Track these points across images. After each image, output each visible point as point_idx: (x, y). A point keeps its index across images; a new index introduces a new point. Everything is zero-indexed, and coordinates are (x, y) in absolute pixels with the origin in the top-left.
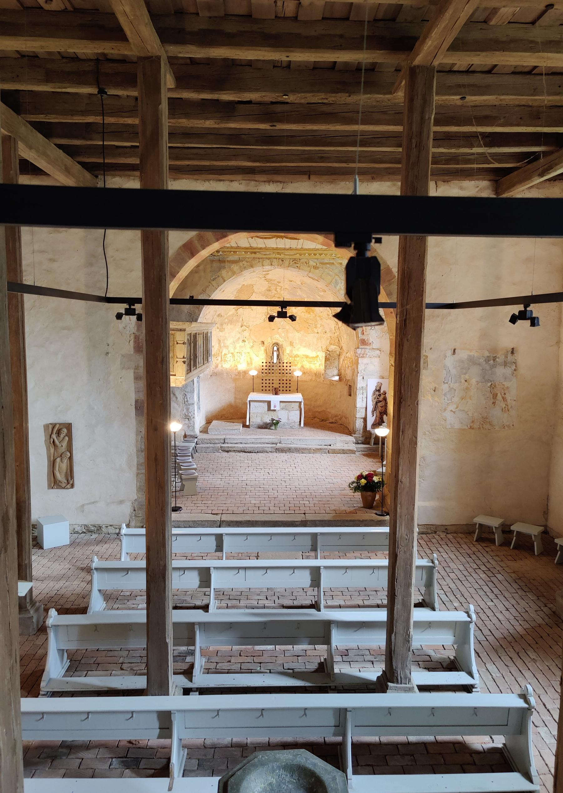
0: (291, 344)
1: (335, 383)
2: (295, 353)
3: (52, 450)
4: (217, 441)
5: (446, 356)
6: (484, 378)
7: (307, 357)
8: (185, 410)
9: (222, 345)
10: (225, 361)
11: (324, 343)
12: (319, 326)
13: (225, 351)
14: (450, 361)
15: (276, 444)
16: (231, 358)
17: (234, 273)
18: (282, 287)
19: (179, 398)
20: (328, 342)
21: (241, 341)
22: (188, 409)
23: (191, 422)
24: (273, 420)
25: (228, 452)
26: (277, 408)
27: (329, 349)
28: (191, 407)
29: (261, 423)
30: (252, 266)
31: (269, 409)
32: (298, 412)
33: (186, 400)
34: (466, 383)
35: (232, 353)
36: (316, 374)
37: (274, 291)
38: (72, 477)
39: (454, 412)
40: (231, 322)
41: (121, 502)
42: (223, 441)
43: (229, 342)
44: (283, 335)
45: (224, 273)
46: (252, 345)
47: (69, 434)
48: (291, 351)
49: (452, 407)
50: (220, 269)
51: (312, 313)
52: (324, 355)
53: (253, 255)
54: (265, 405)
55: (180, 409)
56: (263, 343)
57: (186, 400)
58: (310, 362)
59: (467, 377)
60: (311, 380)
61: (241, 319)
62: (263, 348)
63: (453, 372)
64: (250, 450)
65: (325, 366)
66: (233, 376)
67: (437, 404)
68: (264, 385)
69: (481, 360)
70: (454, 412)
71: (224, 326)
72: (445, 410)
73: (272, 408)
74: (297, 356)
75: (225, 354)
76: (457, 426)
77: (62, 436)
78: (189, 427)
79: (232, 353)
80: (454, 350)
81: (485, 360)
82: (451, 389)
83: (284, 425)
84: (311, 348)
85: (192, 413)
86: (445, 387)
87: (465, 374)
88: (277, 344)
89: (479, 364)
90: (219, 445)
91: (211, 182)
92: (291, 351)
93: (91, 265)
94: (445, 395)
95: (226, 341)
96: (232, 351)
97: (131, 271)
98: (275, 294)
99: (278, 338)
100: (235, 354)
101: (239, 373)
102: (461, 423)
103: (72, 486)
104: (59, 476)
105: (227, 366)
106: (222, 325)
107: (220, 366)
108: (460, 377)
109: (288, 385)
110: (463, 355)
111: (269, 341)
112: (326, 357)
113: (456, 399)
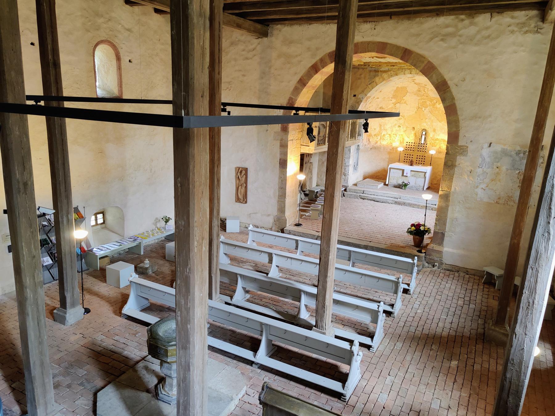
0: (434, 130)
2: (436, 137)
3: (238, 182)
5: (483, 148)
6: (513, 166)
10: (384, 139)
14: (486, 152)
15: (397, 198)
17: (384, 80)
21: (397, 126)
24: (403, 182)
25: (364, 199)
26: (408, 175)
29: (396, 184)
30: (397, 75)
31: (403, 175)
32: (423, 179)
34: (497, 169)
38: (246, 198)
39: (484, 190)
41: (269, 215)
43: (387, 127)
45: (377, 79)
47: (246, 174)
48: (434, 136)
49: (483, 186)
50: (375, 77)
53: (392, 67)
54: (401, 172)
59: (499, 164)
62: (413, 132)
63: (488, 160)
64: (378, 200)
66: (388, 150)
67: (471, 182)
68: (406, 158)
69: (513, 153)
70: (484, 190)
72: (477, 187)
73: (405, 174)
74: (437, 139)
75: (384, 135)
76: (486, 200)
77: (242, 174)
80: (490, 144)
81: (516, 153)
82: (484, 172)
83: (412, 187)
86: (480, 171)
87: (498, 162)
88: (425, 130)
89: (511, 156)
90: (359, 194)
91: (331, 25)
92: (434, 136)
93: (262, 78)
94: (479, 176)
96: (390, 133)
97: (282, 82)
99: (425, 126)
100: (392, 135)
102: (489, 198)
103: (246, 202)
104: (241, 197)
105: (384, 143)
107: (379, 143)
108: (493, 164)
109: (423, 160)
110: (498, 148)
111: (418, 128)
113: (487, 181)
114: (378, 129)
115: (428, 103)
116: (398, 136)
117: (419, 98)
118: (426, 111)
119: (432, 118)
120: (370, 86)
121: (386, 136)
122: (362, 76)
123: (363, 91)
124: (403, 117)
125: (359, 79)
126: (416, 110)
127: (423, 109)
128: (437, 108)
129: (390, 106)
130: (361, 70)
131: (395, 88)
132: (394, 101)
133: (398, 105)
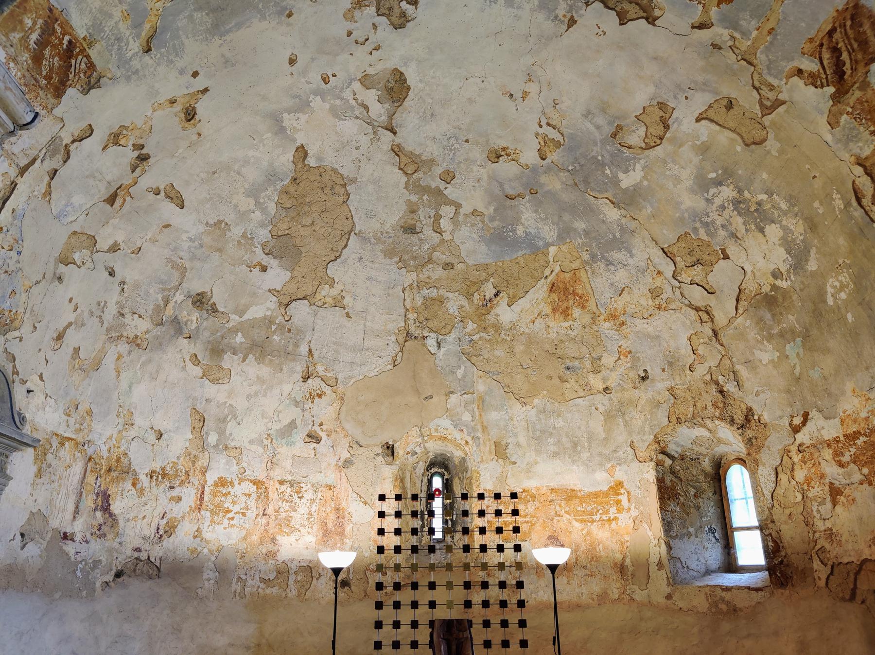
0: (500, 451)
1: (742, 601)
7: (570, 495)
9: (213, 439)
10: (218, 510)
11: (643, 425)
12: (608, 360)
13: (220, 467)
16: (252, 503)
18: (458, 206)
20: (662, 417)
21: (299, 436)
27: (672, 449)
35: (257, 483)
36: (621, 569)
37: (428, 232)
40: (259, 349)
43: (243, 433)
44: (467, 417)
46: (345, 455)
48: (502, 478)
51: (576, 312)
52: (649, 474)
56: (390, 450)
58: (586, 518)
60: (603, 598)
61: (303, 349)
65: (667, 526)
66: (253, 584)
71: (228, 361)
75: (222, 482)
79: (257, 483)
84: (585, 455)
88: (440, 464)
92: (502, 478)
95: (231, 427)
96: (261, 475)
98: (434, 249)
99: (444, 430)
100: (273, 486)
101: (283, 572)
105: (225, 534)
106: (217, 351)
111: (415, 447)
112: (660, 481)
115: (455, 303)
116: (309, 495)
117: (410, 278)
118: (445, 352)
119: (481, 387)
121: (237, 490)
124: (333, 383)
126: (394, 348)
127: (431, 342)
128: (498, 328)
129: (256, 312)
132: (277, 276)
133: (301, 311)
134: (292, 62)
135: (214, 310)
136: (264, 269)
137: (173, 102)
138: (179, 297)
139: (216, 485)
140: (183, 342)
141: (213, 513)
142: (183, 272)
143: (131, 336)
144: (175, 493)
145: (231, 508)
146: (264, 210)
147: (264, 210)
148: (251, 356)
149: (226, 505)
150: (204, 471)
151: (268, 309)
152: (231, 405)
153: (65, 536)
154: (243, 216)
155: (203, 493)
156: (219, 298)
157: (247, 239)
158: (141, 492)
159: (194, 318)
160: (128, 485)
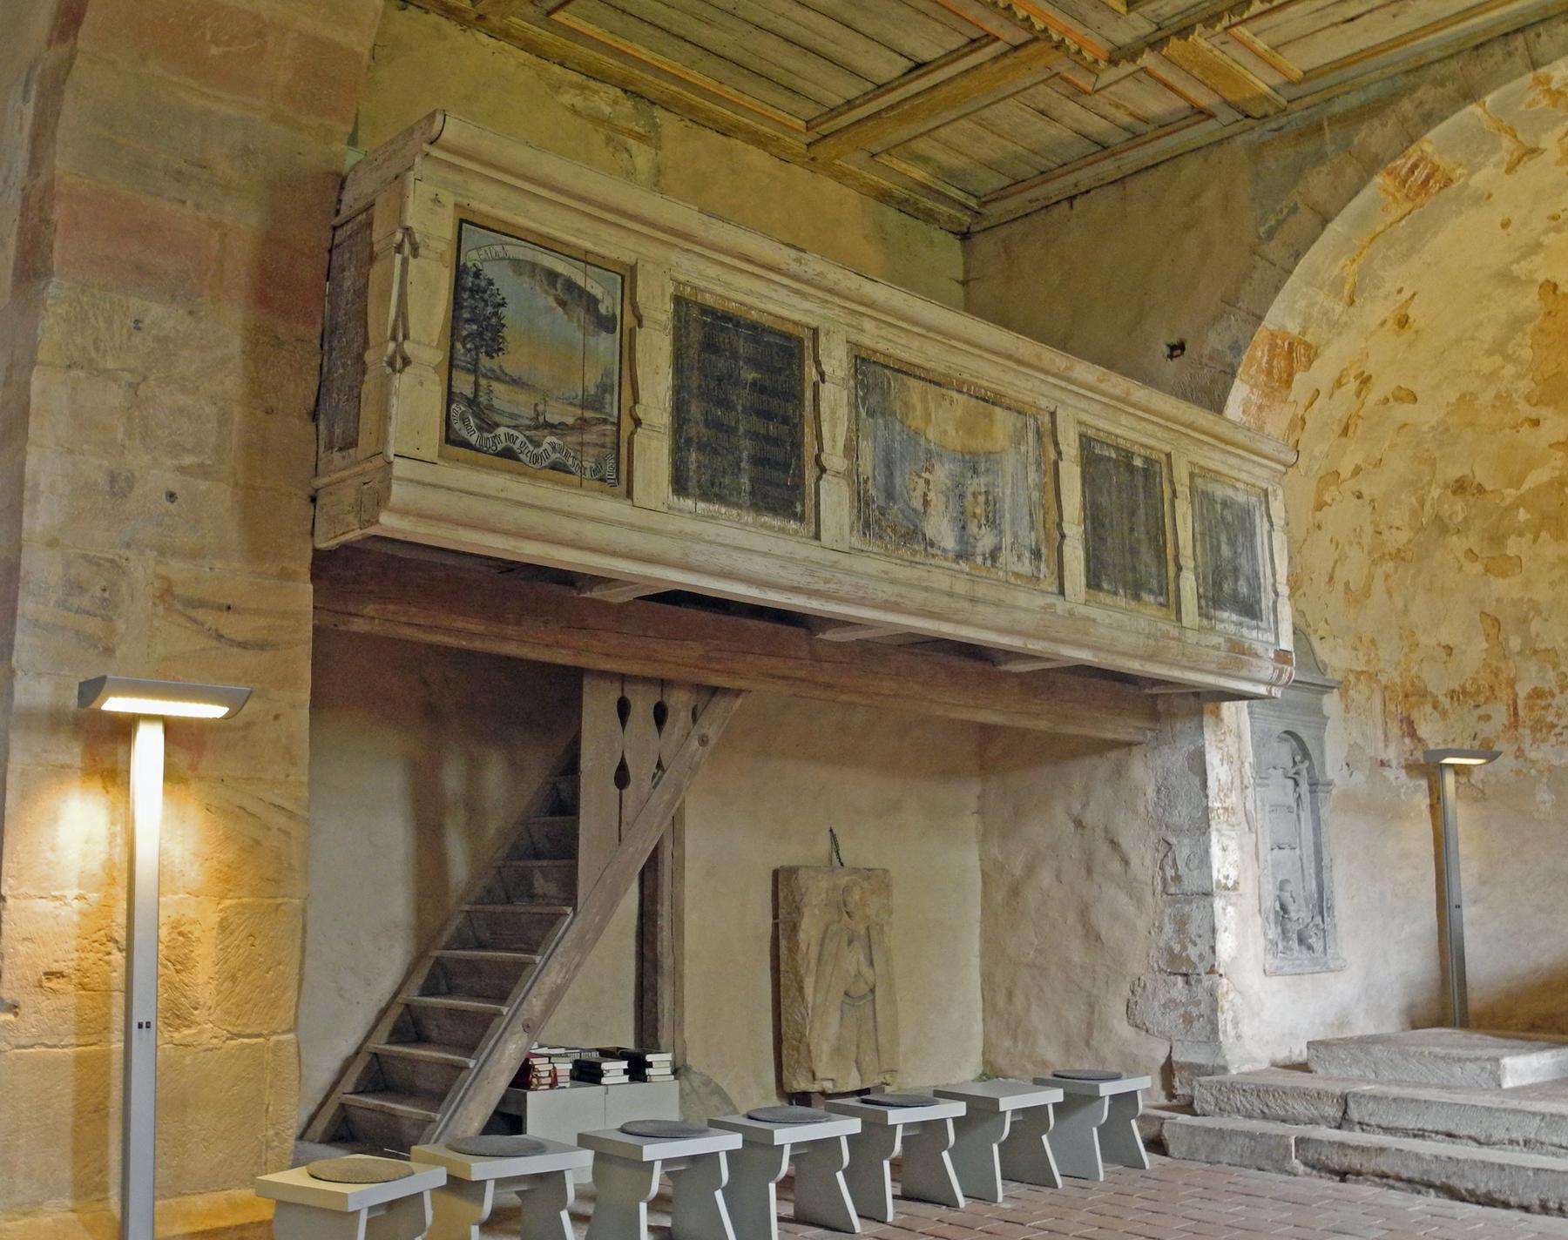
4: (1300, 1108)
8: (1169, 929)
9: (1515, 643)
19: (1135, 861)
22: (1181, 923)
23: (1201, 993)
25: (1343, 1175)
28: (1195, 912)
33: (1170, 872)
42: (1333, 1112)
45: (1318, 184)
50: (1297, 172)
55: (1142, 924)
57: (1170, 872)
71: (1513, 546)
75: (1537, 694)
78: (1188, 1020)
85: (1203, 947)
90: (1293, 1132)
106: (1496, 539)
114: (1474, 652)
120: (1274, 250)
122: (1209, 199)
123: (1230, 301)
125: (1187, 227)
129: (1538, 477)
130: (1191, 169)
131: (1530, 300)
134: (1505, 225)
135: (1480, 489)
136: (1536, 423)
137: (1383, 323)
138: (1435, 492)
139: (1530, 697)
140: (1454, 540)
141: (1534, 730)
142: (1433, 463)
143: (1394, 551)
144: (1480, 711)
145: (1556, 721)
146: (1516, 361)
147: (1516, 361)
148: (1543, 534)
149: (1549, 719)
150: (1512, 683)
151: (1554, 468)
152: (1530, 600)
153: (1382, 763)
154: (1491, 378)
155: (1515, 708)
156: (1482, 477)
157: (1503, 401)
158: (1444, 714)
159: (1458, 508)
160: (1428, 708)
